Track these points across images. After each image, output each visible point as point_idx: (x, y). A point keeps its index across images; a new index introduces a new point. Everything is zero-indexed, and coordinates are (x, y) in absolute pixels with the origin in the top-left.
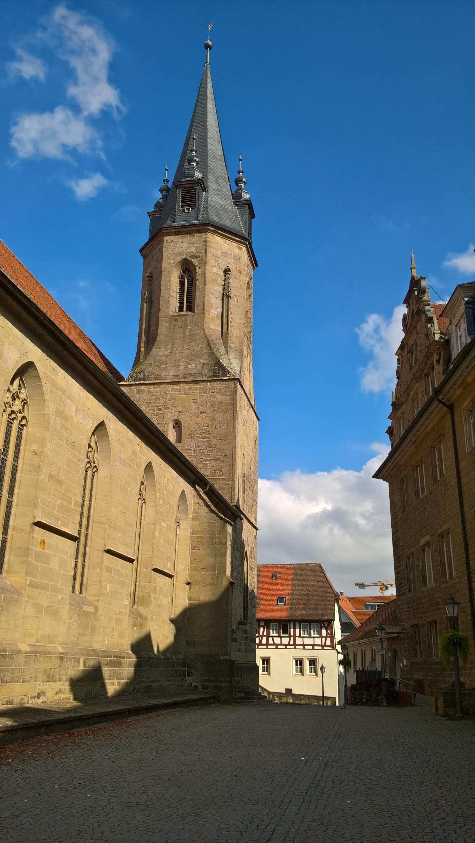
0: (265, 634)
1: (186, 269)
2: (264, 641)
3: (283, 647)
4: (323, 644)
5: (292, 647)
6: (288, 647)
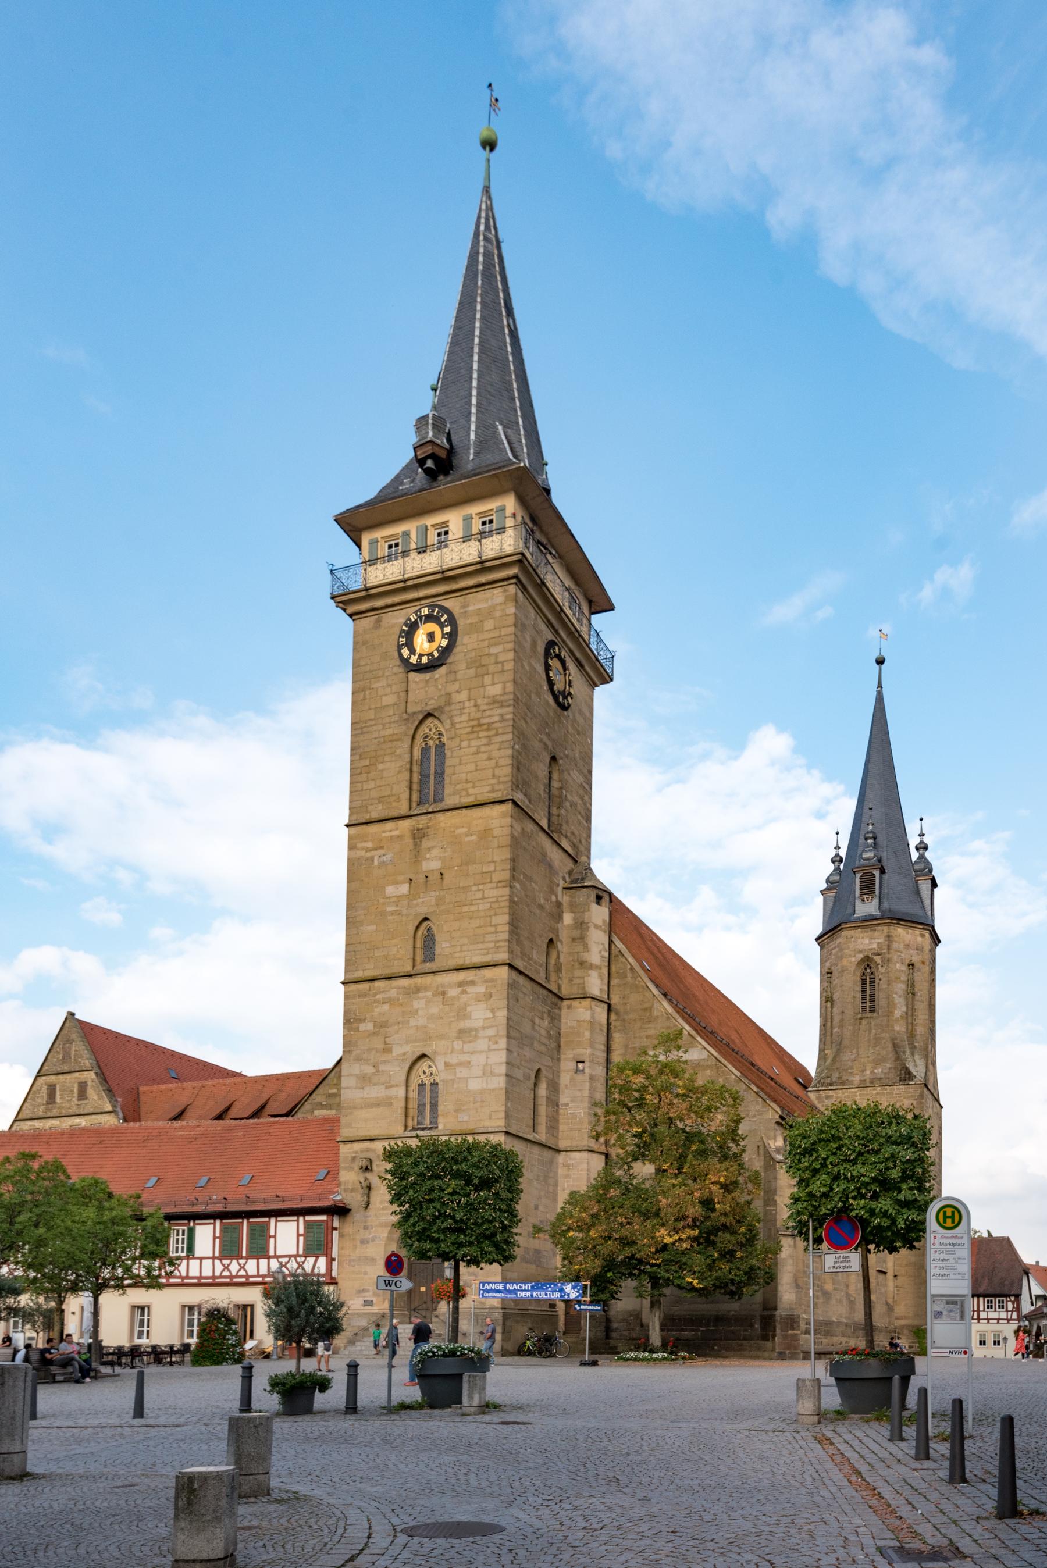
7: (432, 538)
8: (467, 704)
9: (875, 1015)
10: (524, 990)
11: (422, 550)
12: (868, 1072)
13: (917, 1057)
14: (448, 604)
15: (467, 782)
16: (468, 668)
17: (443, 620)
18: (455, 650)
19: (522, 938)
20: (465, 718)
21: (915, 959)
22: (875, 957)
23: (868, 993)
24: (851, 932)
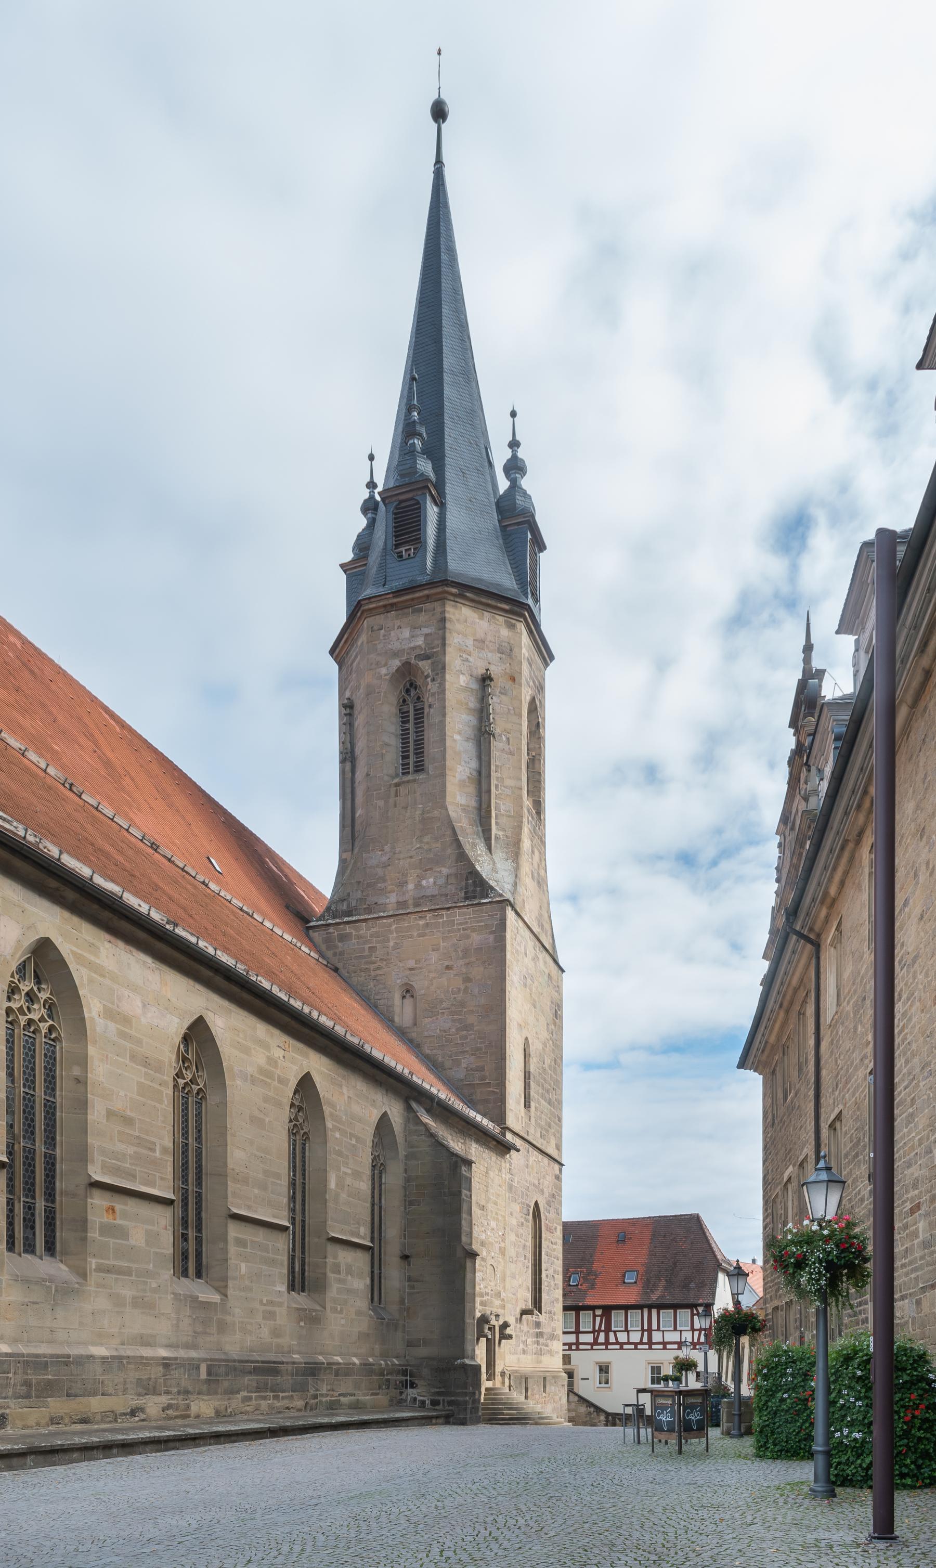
0: (603, 1328)
1: (411, 685)
2: (602, 1339)
3: (632, 1347)
4: (696, 1340)
5: (647, 1347)
6: (639, 1347)
9: (422, 776)
12: (411, 886)
13: (499, 855)
21: (495, 670)
22: (420, 664)
23: (412, 737)
24: (378, 620)
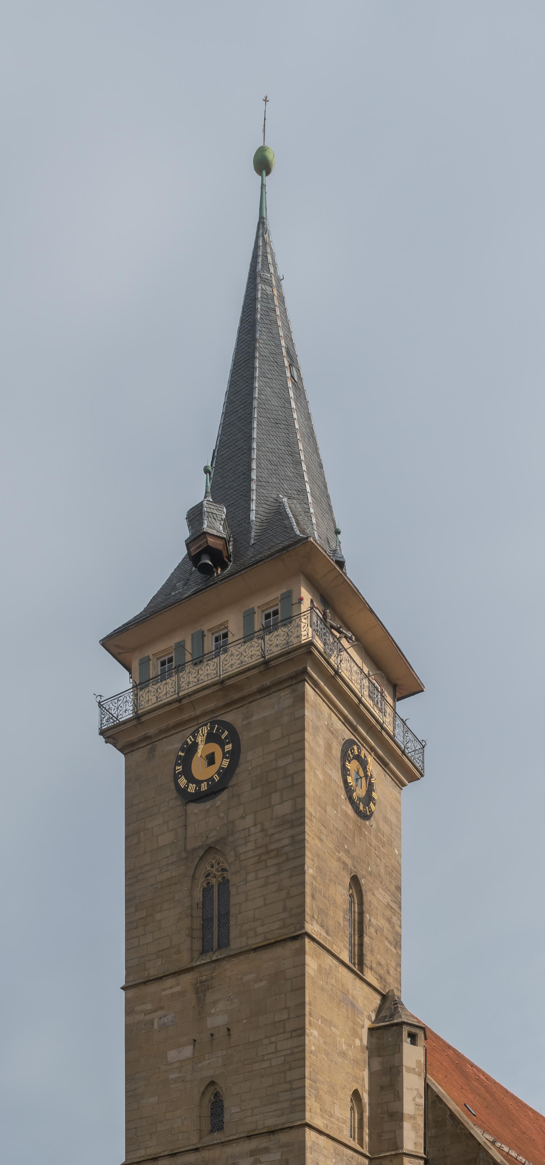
7: (209, 644)
8: (253, 830)
10: (325, 1152)
11: (198, 661)
14: (228, 718)
15: (255, 920)
16: (253, 788)
17: (223, 737)
18: (238, 770)
19: (321, 1093)
20: (251, 846)
